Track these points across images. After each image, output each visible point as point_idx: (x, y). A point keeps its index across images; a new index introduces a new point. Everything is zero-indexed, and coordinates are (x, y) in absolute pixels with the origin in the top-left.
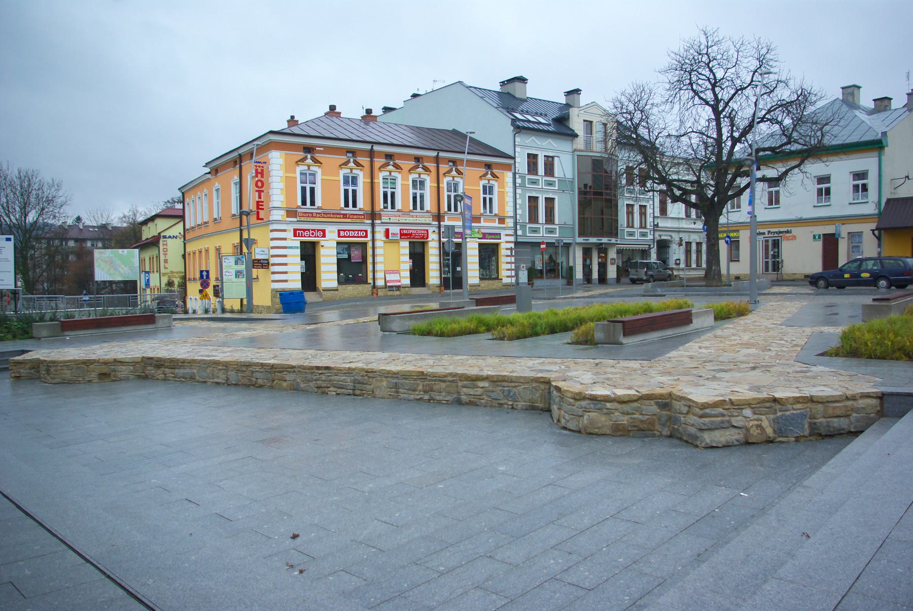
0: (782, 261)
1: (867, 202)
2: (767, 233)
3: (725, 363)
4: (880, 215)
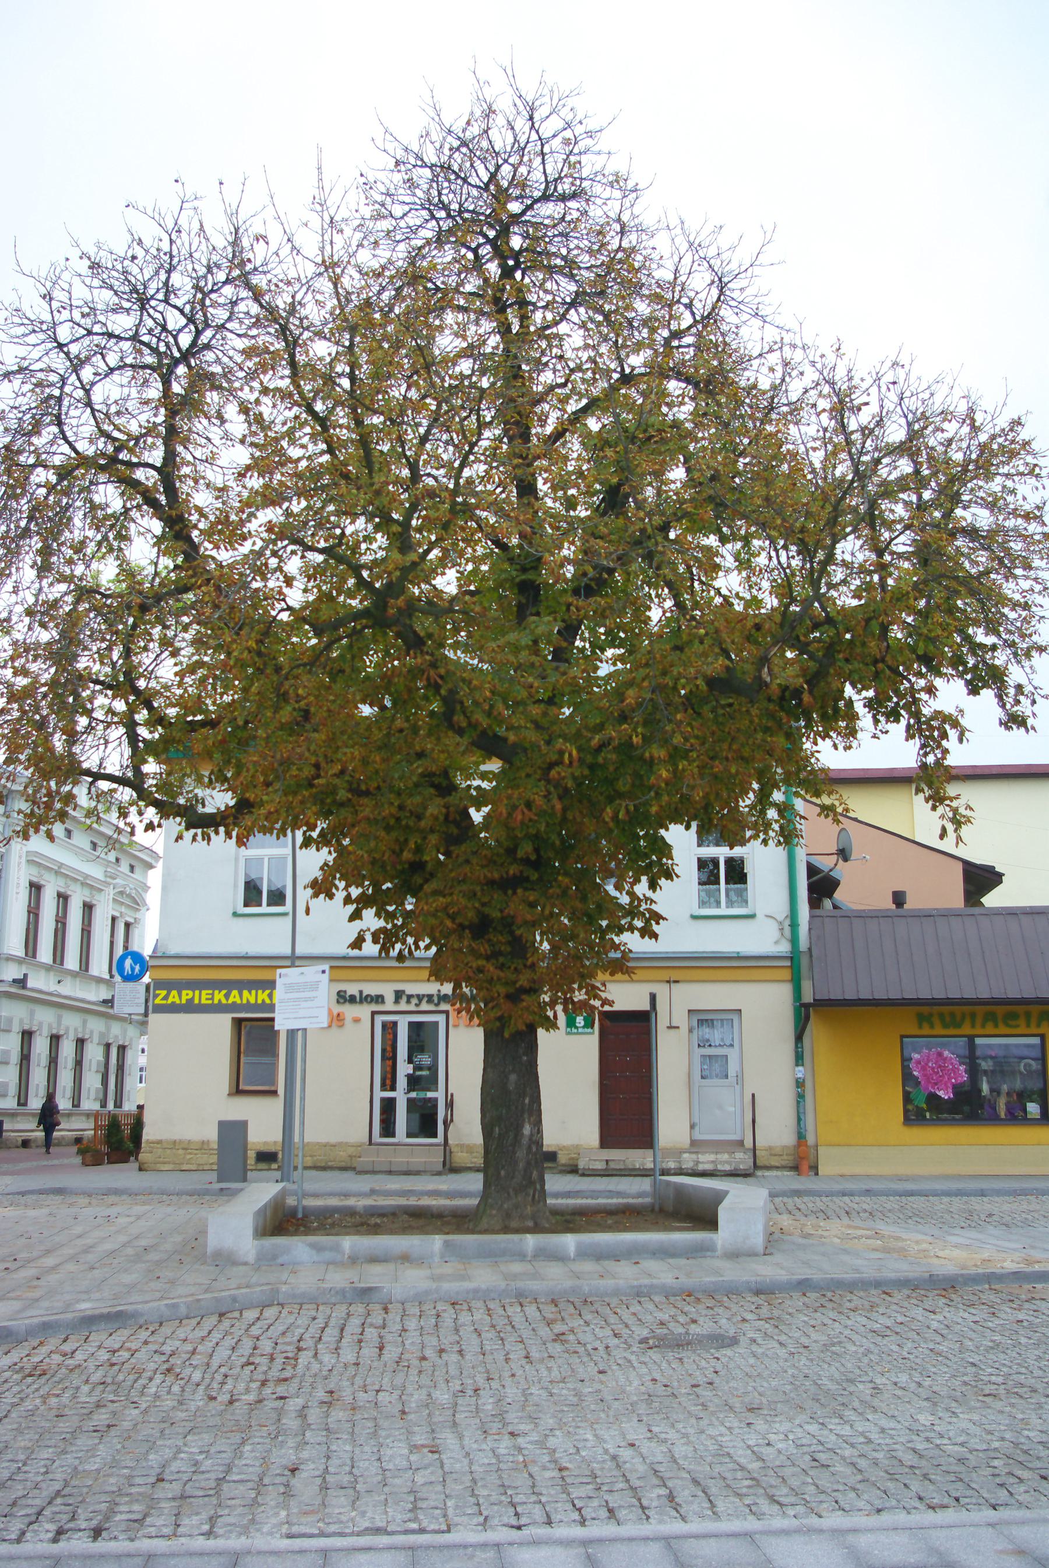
0: (450, 1105)
1: (752, 916)
2: (390, 998)
3: (201, 1493)
4: (793, 957)
